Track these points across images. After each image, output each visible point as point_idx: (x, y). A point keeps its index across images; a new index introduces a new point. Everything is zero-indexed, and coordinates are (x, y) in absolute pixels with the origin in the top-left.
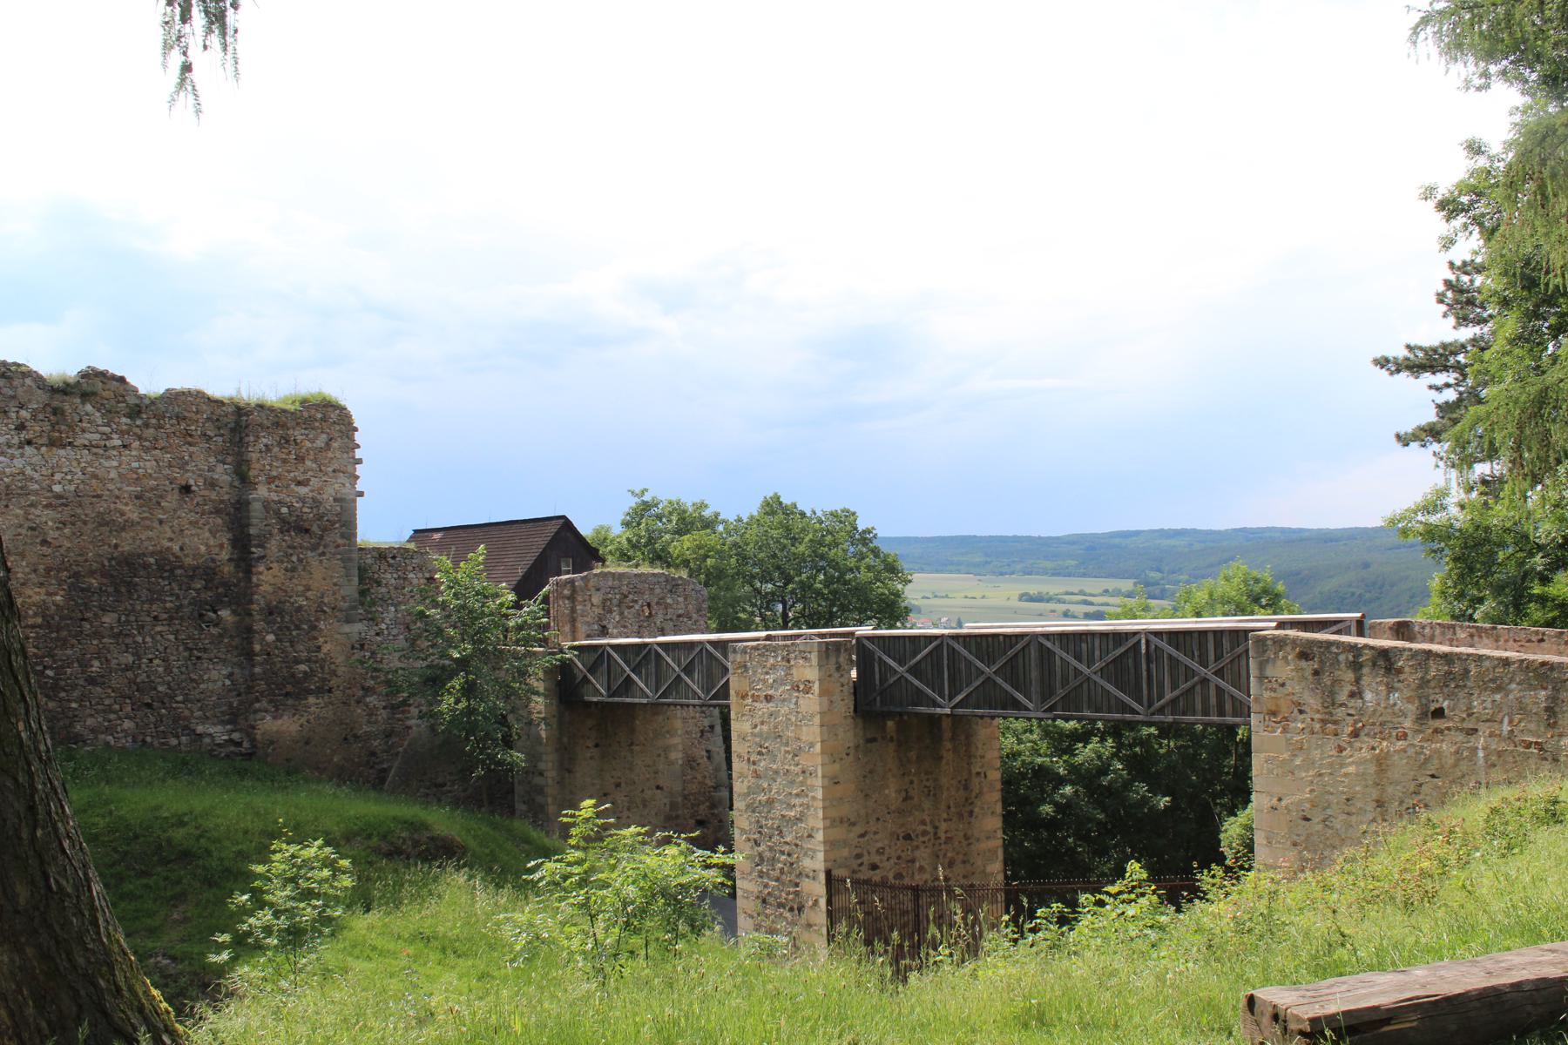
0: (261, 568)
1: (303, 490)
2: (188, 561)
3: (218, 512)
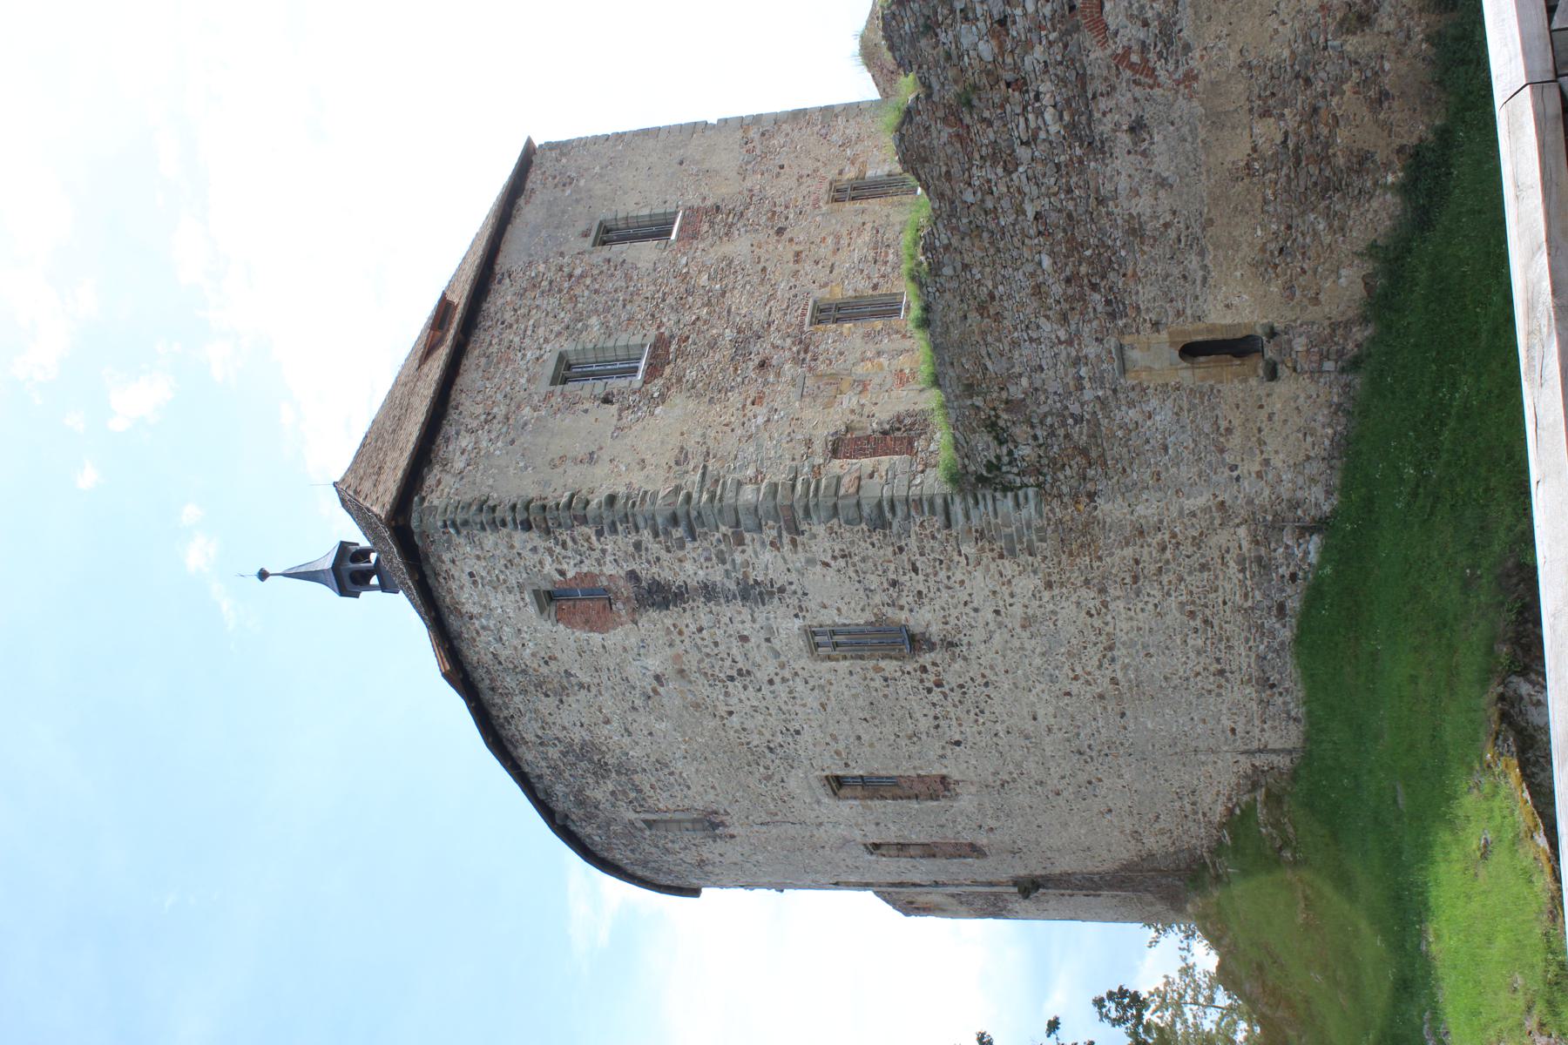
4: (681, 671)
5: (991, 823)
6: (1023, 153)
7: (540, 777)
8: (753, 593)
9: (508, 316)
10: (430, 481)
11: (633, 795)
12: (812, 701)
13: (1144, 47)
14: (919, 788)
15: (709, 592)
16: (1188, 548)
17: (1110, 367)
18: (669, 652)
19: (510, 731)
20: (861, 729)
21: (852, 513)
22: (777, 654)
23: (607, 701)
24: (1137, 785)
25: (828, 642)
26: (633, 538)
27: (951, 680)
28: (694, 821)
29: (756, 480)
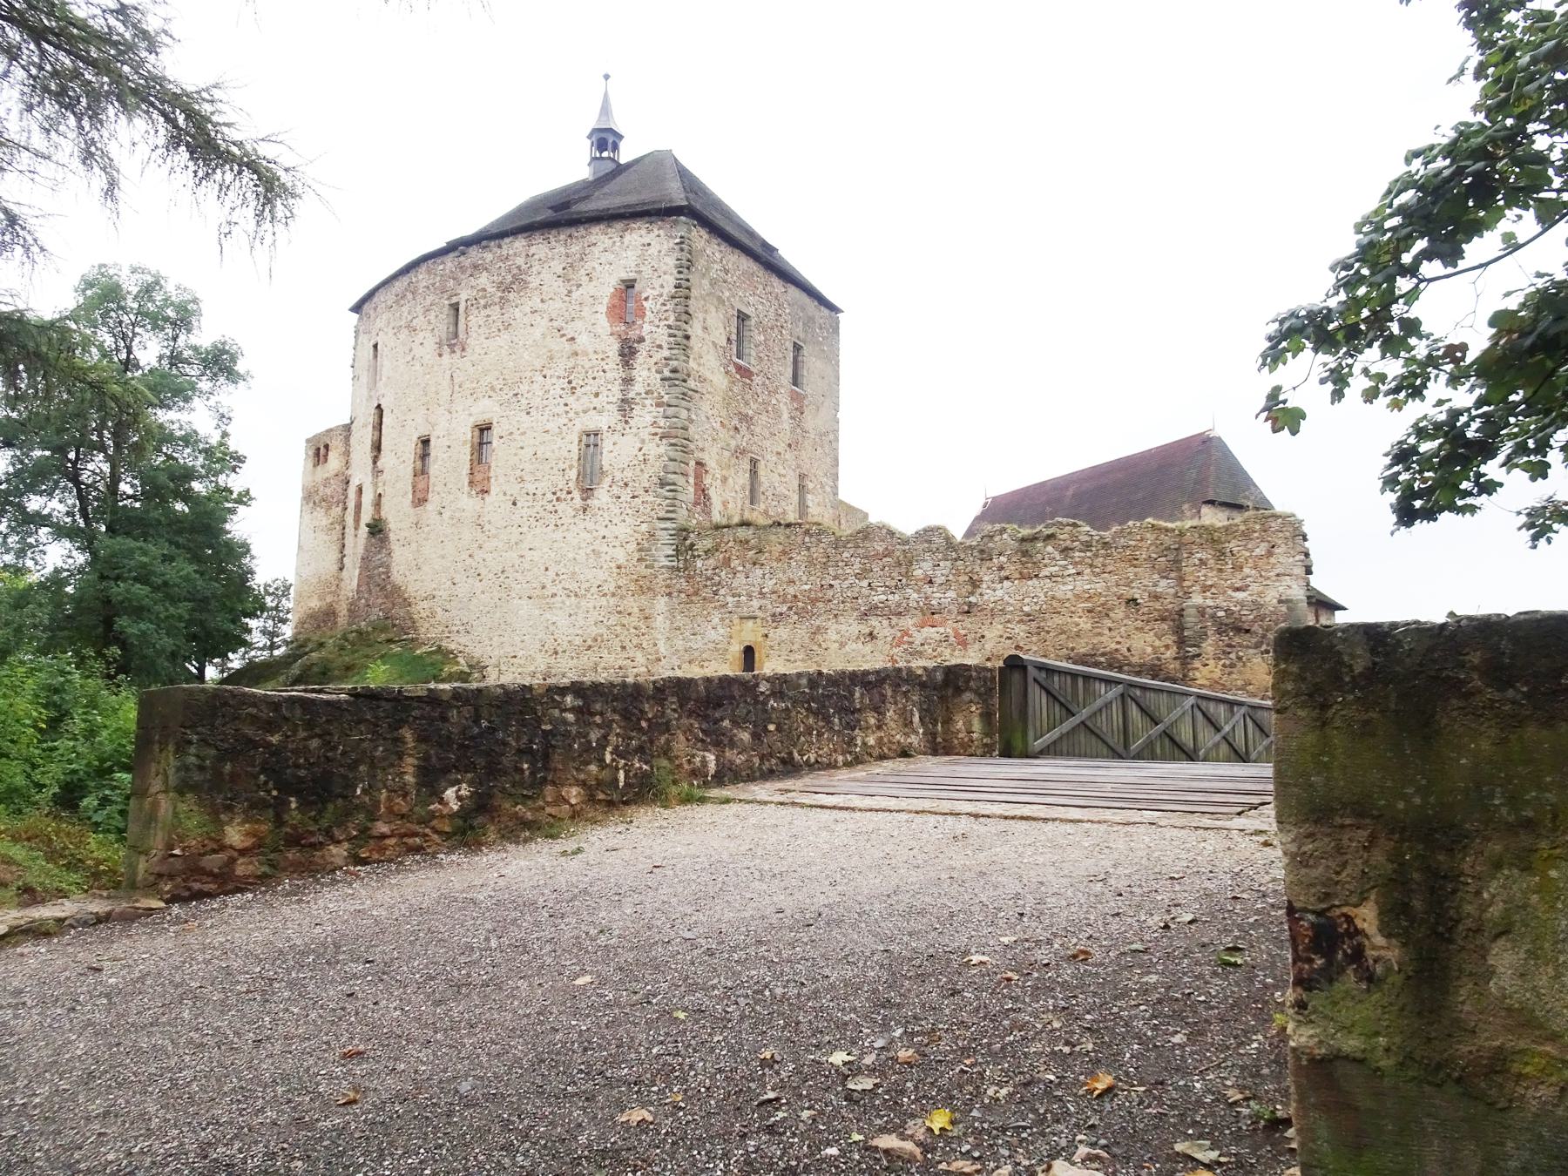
0: (1197, 663)
1: (1240, 595)
2: (1135, 660)
3: (1163, 619)
4: (577, 354)
5: (447, 514)
6: (865, 583)
7: (500, 247)
8: (626, 406)
9: (769, 289)
10: (703, 232)
11: (482, 302)
12: (551, 426)
13: (911, 643)
14: (478, 477)
15: (628, 381)
16: (635, 641)
17: (745, 611)
18: (591, 351)
19: (538, 238)
20: (528, 452)
21: (671, 469)
22: (585, 412)
23: (558, 304)
24: (475, 601)
25: (591, 440)
26: (665, 346)
27: (561, 507)
28: (456, 335)
29: (692, 421)
